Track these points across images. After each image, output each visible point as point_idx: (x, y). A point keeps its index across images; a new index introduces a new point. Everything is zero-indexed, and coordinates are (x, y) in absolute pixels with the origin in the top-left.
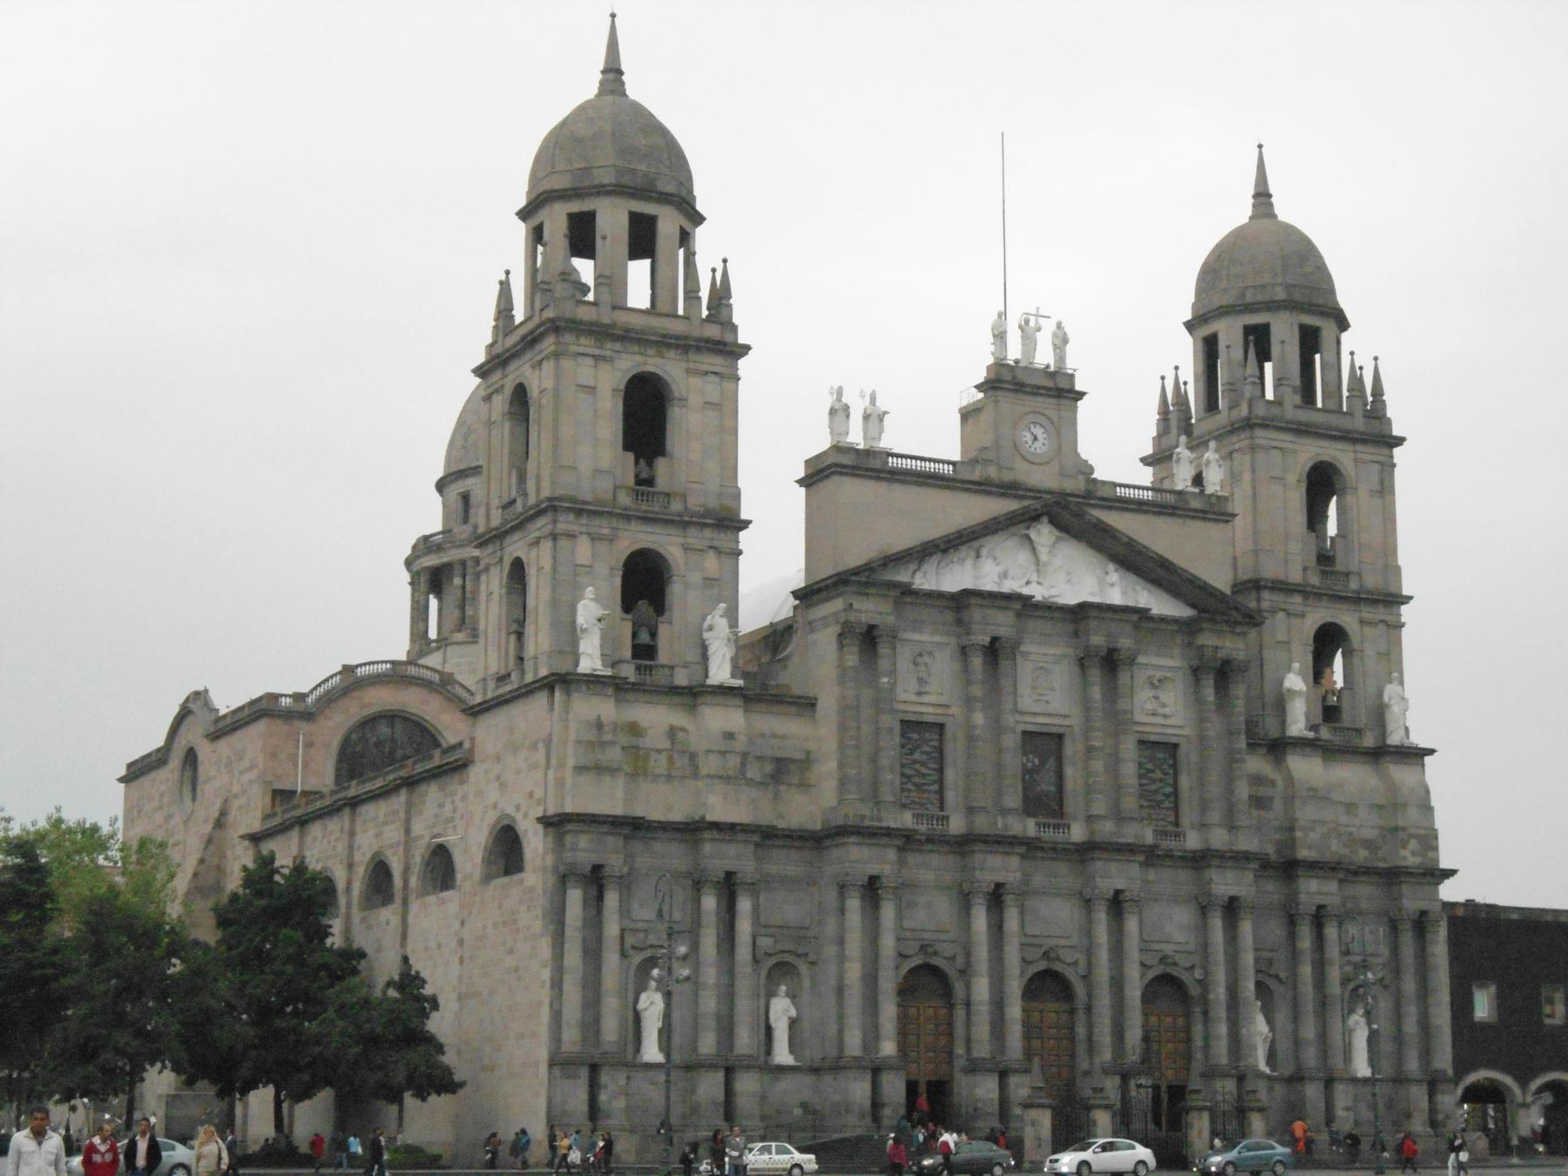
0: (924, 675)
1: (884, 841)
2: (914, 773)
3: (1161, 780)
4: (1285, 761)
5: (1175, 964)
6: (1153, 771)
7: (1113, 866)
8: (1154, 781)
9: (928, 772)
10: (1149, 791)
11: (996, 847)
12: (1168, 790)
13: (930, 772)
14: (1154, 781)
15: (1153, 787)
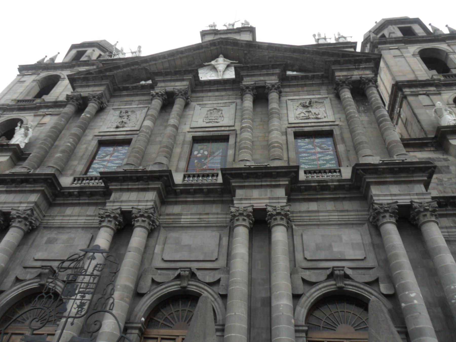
0: (125, 120)
1: (28, 187)
2: (101, 166)
3: (319, 153)
4: (451, 144)
5: (347, 277)
6: (314, 149)
7: (256, 193)
8: (315, 154)
9: (113, 165)
10: (310, 160)
11: (131, 185)
12: (328, 157)
13: (113, 165)
14: (315, 154)
15: (314, 157)
